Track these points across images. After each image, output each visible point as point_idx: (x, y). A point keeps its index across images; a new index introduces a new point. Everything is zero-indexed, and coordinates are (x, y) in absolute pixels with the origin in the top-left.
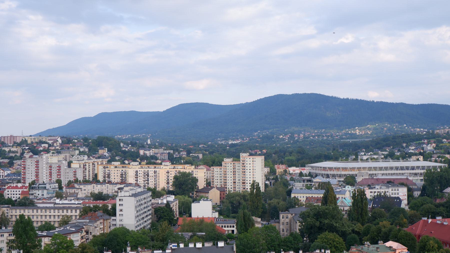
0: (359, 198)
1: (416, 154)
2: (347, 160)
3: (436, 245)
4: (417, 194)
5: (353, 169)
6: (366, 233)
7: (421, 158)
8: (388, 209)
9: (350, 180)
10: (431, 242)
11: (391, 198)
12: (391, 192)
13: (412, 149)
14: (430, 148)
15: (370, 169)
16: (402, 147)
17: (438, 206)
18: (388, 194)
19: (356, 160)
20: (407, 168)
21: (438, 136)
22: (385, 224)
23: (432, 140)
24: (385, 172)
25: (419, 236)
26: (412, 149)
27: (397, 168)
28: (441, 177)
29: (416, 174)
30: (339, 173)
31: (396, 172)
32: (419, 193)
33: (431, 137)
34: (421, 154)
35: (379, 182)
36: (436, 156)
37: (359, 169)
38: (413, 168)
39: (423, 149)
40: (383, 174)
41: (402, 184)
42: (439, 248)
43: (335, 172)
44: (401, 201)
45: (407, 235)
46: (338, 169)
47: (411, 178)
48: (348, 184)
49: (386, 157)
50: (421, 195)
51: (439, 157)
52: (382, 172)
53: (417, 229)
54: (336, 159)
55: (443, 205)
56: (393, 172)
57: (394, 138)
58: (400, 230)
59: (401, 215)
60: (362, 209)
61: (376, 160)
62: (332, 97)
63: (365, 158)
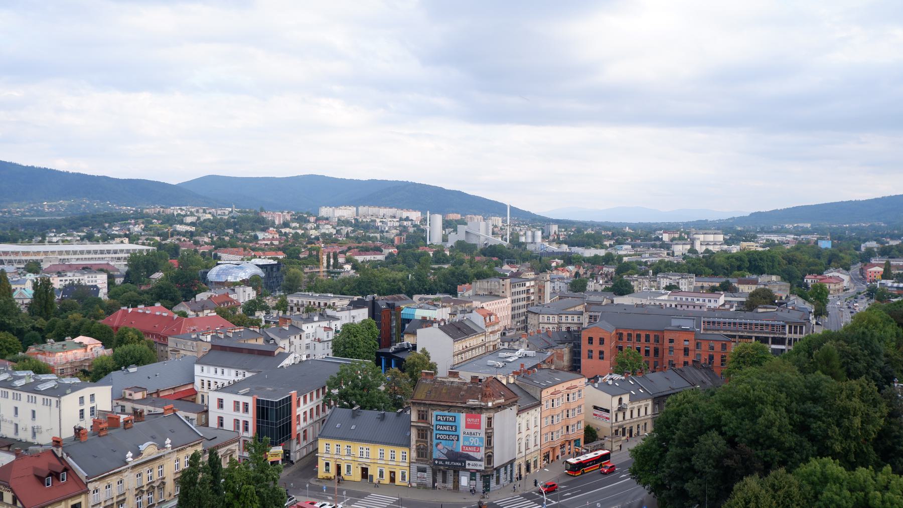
0: (43, 290)
1: (120, 236)
2: (30, 242)
3: (136, 337)
4: (119, 281)
5: (38, 253)
6: (50, 329)
7: (126, 240)
8: (80, 299)
9: (33, 267)
10: (130, 333)
11: (86, 286)
12: (87, 280)
13: (116, 230)
14: (137, 229)
15: (60, 253)
16: (104, 228)
17: (140, 294)
18: (83, 282)
19: (42, 242)
20: (109, 252)
21: (148, 216)
22: (75, 317)
23: (140, 221)
24: (80, 256)
25: (117, 328)
26: (116, 230)
27: (96, 252)
28: (148, 261)
29: (119, 259)
30: (18, 258)
31: (94, 256)
32: (122, 279)
33: (138, 217)
34: (126, 236)
35: (71, 268)
36: (143, 238)
37: (46, 253)
38: (115, 252)
39: (129, 230)
40: (78, 259)
41: (101, 271)
42: (140, 339)
43: (13, 258)
44: (98, 290)
45: (102, 327)
46: (17, 253)
47: (112, 263)
48: (30, 271)
49: (82, 239)
50: (124, 282)
51: (147, 239)
52: (77, 256)
53: (114, 320)
54: (14, 241)
55: (147, 293)
56: (90, 256)
57: (94, 217)
58: (93, 323)
59: (97, 306)
60: (47, 302)
61: (70, 242)
62: (11, 164)
63: (55, 239)
